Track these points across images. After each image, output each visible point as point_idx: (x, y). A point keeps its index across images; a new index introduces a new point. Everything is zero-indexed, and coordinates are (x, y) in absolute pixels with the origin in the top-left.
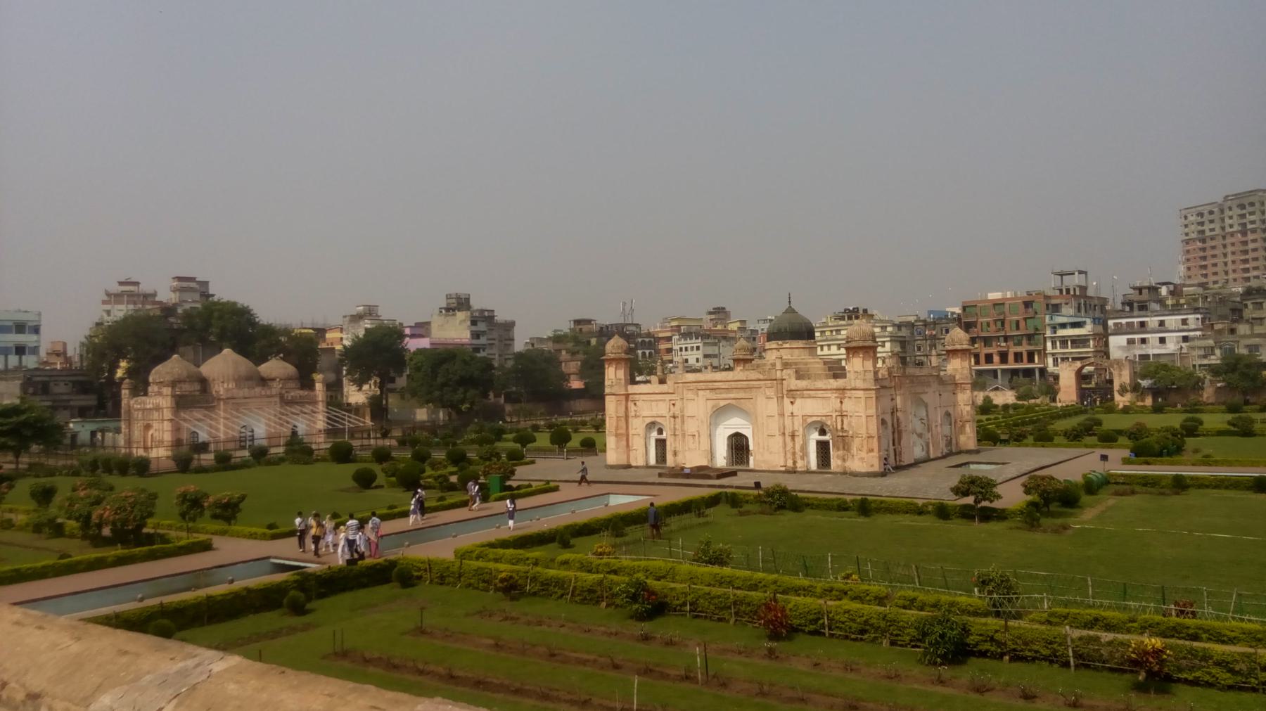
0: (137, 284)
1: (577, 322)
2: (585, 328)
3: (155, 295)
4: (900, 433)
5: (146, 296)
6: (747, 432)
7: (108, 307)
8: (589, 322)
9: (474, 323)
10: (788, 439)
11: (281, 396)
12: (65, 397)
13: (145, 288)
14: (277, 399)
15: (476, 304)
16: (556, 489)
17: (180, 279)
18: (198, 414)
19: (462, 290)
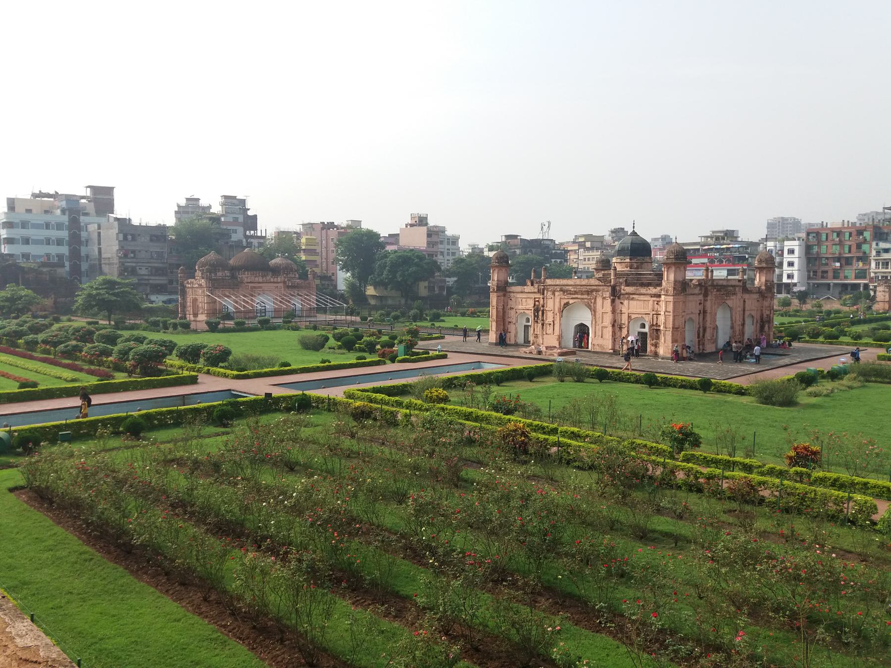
1: (508, 237)
2: (512, 241)
3: (210, 207)
4: (705, 330)
5: (204, 208)
6: (588, 324)
7: (179, 216)
8: (515, 237)
9: (429, 235)
10: (617, 329)
11: (284, 282)
12: (147, 277)
13: (203, 203)
14: (281, 285)
15: (431, 223)
16: (444, 357)
19: (422, 212)
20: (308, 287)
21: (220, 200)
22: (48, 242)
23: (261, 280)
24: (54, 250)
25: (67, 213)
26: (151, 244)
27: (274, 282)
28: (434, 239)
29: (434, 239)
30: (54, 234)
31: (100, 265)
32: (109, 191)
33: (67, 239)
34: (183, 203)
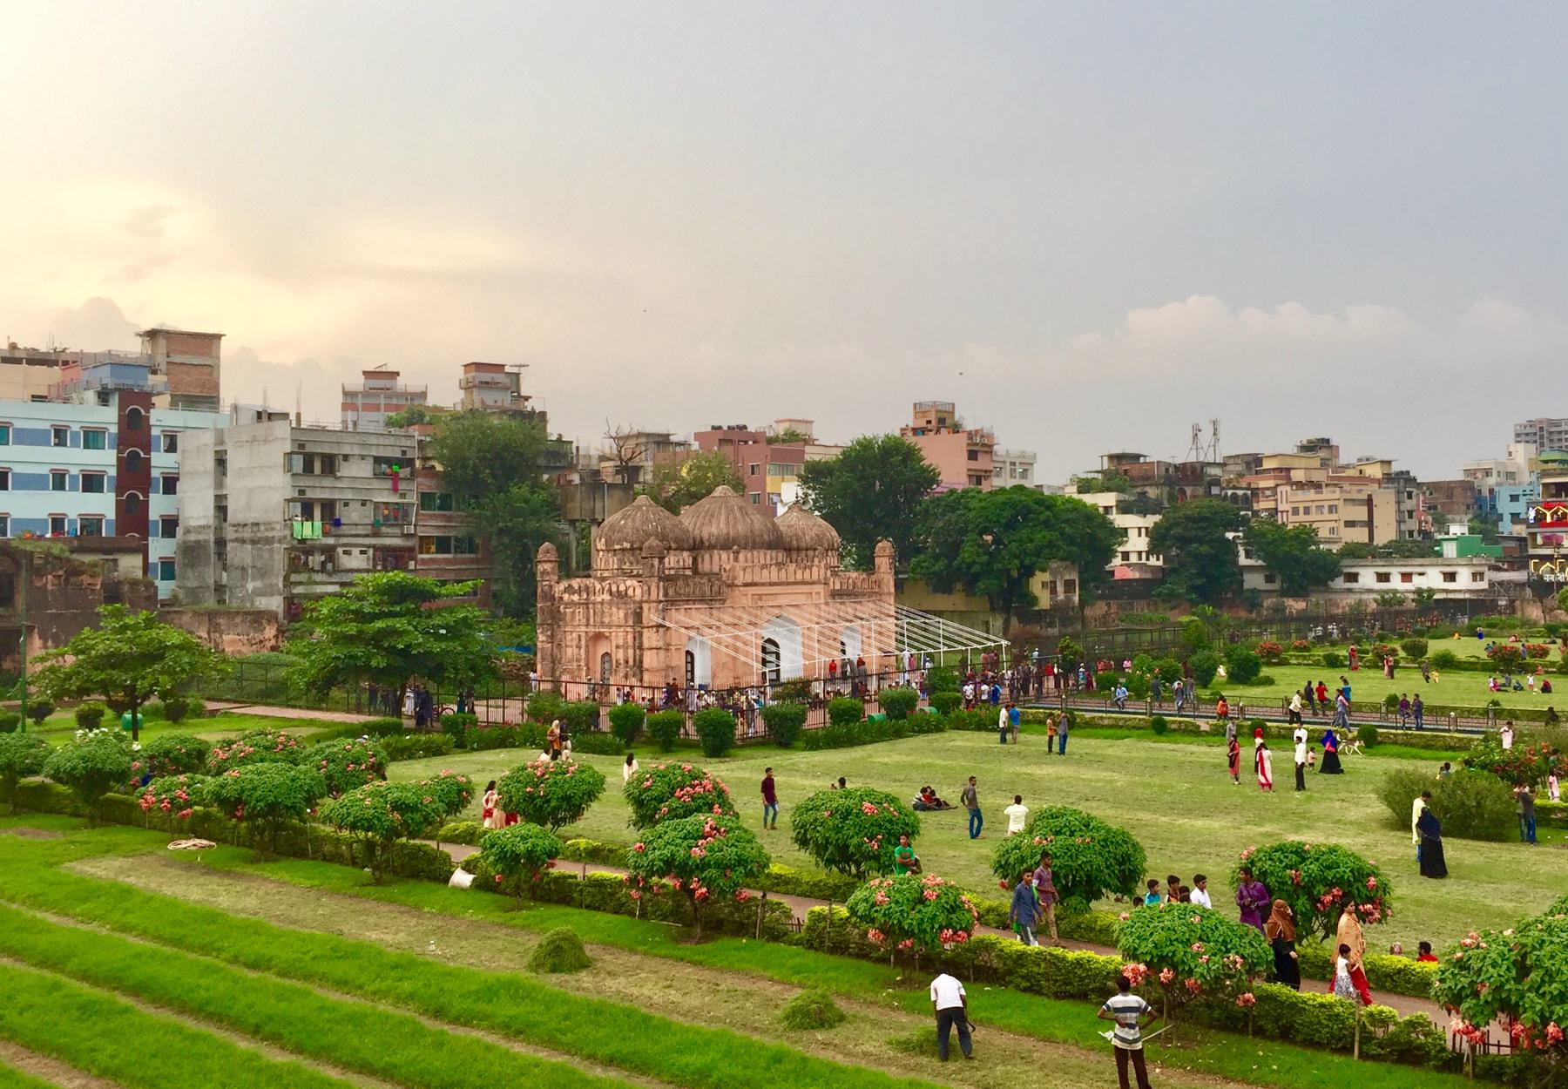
0: (394, 375)
1: (1117, 458)
3: (423, 395)
9: (973, 455)
17: (479, 366)
18: (697, 615)
20: (876, 594)
21: (460, 373)
22: (59, 480)
23: (774, 579)
24: (75, 505)
25: (115, 400)
26: (376, 484)
27: (803, 583)
28: (982, 463)
29: (982, 463)
30: (77, 458)
31: (221, 543)
32: (207, 342)
33: (113, 472)
34: (357, 382)
